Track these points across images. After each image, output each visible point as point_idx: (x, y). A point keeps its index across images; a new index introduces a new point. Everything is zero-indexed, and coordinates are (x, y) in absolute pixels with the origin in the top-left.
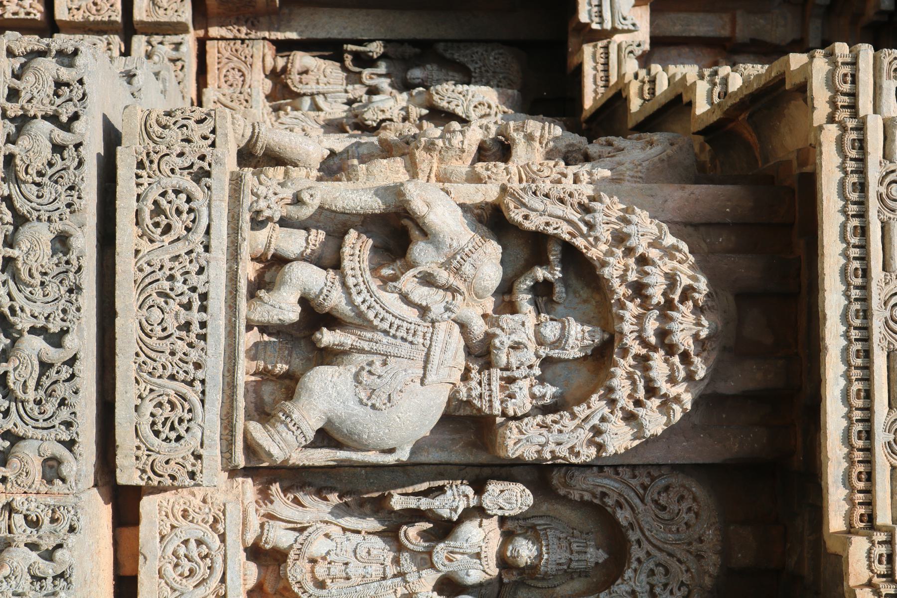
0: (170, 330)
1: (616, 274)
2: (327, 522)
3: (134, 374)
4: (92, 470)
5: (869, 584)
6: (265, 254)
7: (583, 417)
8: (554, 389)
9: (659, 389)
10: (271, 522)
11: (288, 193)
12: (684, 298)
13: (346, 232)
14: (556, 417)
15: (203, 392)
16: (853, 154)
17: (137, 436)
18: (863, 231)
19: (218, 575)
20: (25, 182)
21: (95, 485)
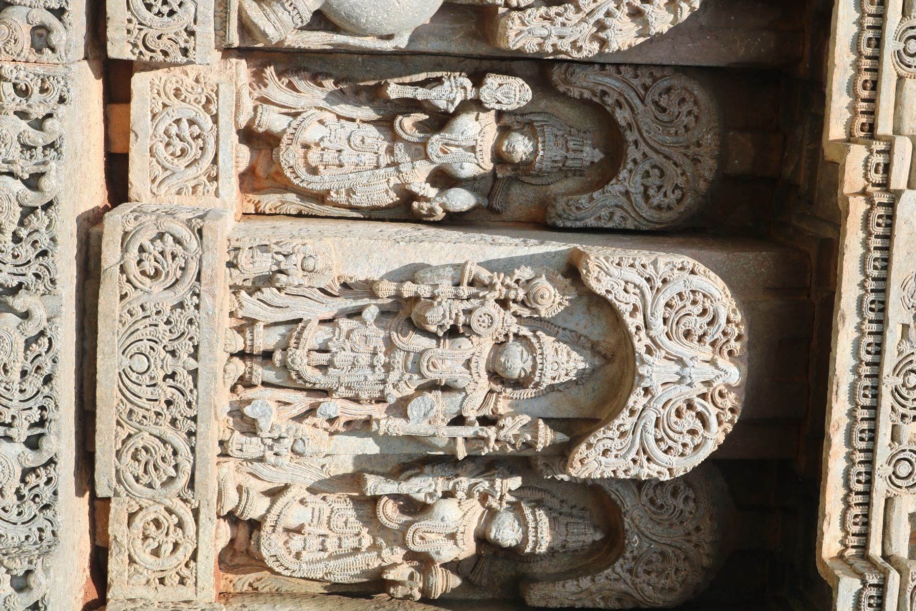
2: (321, 109)
4: (81, 42)
5: (864, 192)
7: (587, 11)
10: (265, 106)
14: (560, 9)
17: (129, 8)
19: (210, 156)
21: (86, 58)
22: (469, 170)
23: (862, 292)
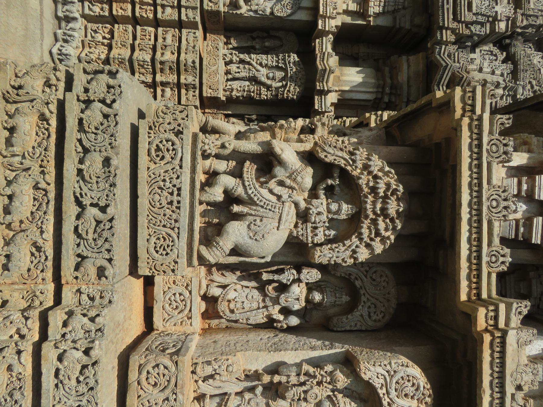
0: (163, 205)
1: (364, 183)
3: (146, 225)
5: (486, 330)
6: (209, 171)
7: (348, 245)
8: (334, 232)
9: (381, 234)
11: (219, 143)
12: (392, 194)
13: (245, 162)
14: (337, 245)
15: (179, 233)
16: (476, 131)
17: (148, 253)
18: (479, 166)
20: (88, 132)
22: (296, 307)
23: (491, 378)
